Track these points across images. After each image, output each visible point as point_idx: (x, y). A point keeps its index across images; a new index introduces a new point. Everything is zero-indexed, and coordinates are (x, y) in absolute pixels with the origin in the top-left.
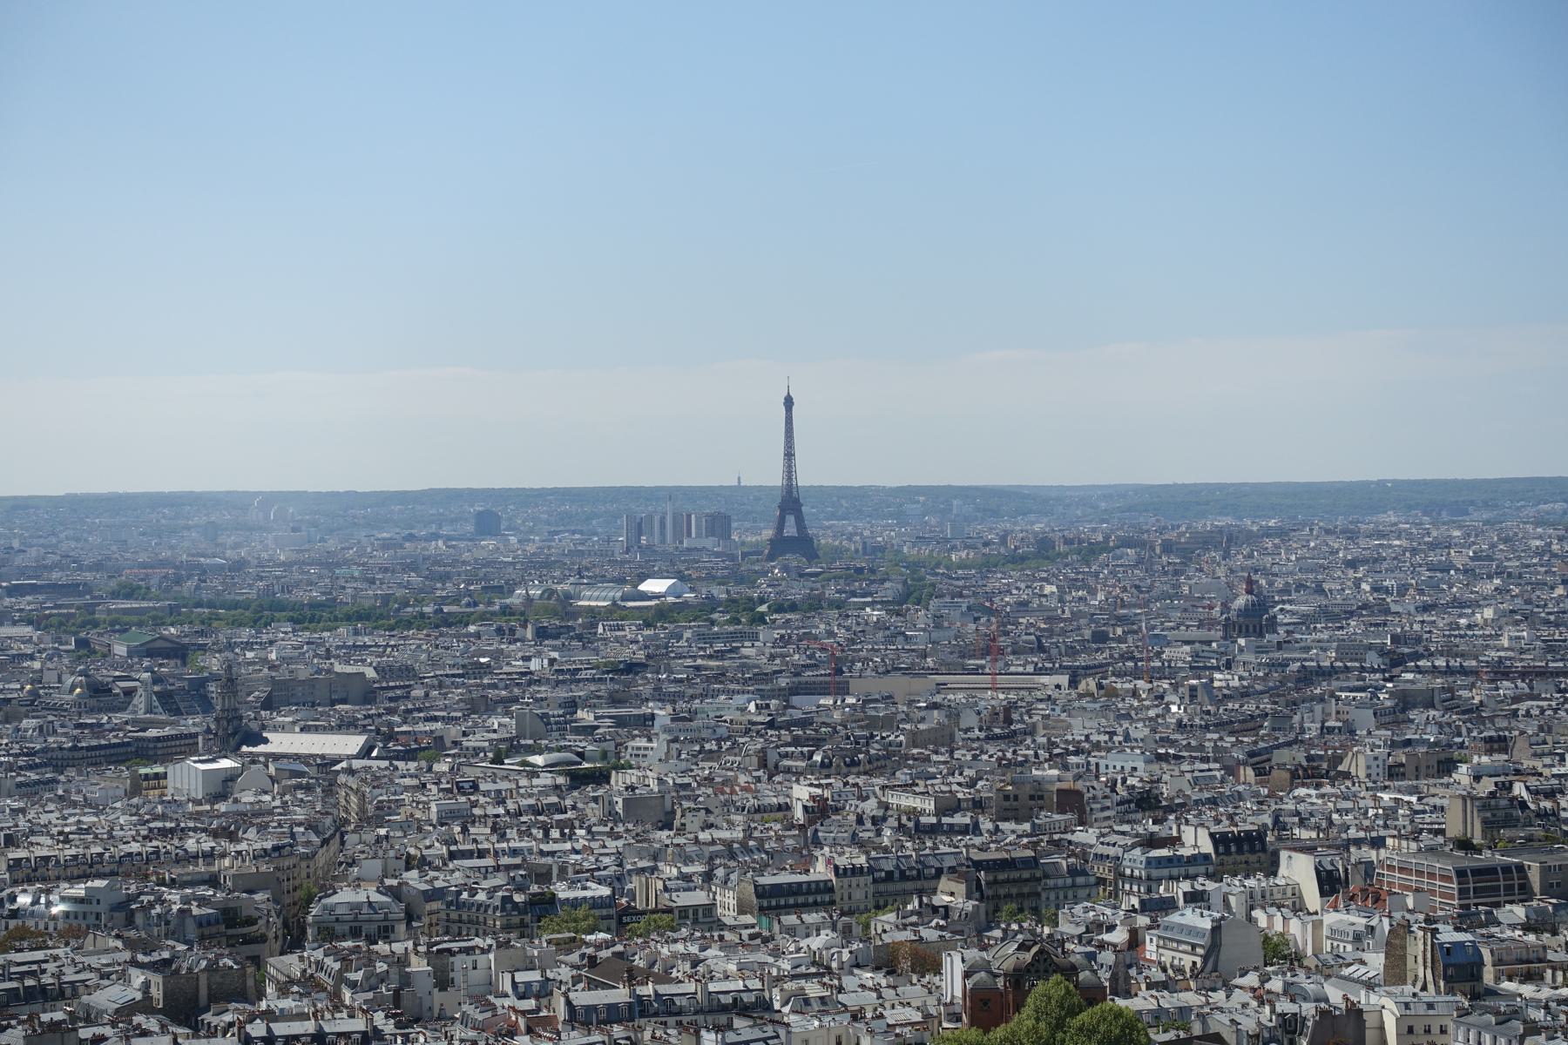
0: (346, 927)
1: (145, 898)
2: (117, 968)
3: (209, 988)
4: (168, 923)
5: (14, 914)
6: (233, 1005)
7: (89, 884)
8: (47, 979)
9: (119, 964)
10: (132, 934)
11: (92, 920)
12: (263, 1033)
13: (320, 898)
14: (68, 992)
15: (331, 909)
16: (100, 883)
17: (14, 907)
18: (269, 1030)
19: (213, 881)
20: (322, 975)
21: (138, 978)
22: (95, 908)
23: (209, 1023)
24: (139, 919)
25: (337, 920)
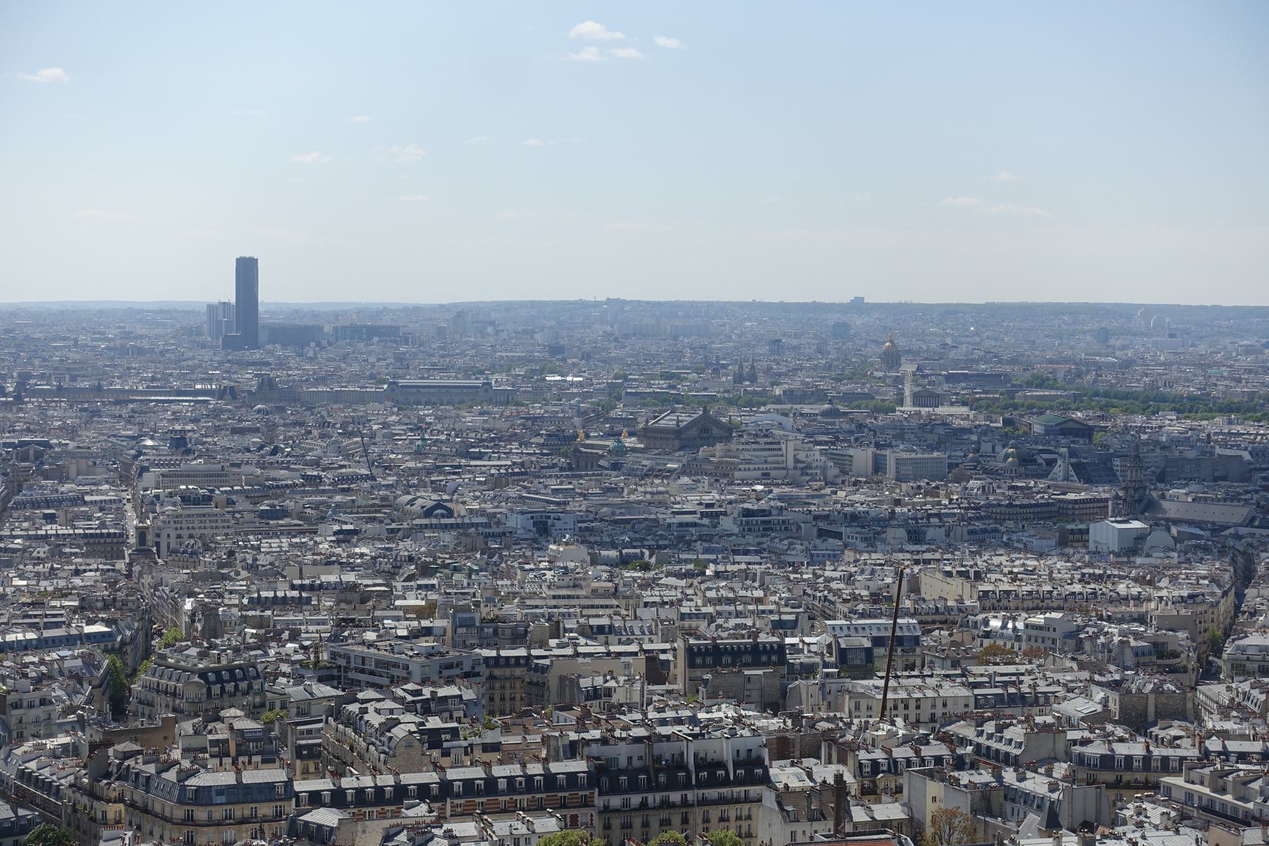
0: (1256, 666)
1: (1091, 630)
2: (1080, 684)
3: (1156, 707)
4: (1110, 651)
5: (987, 635)
6: (1176, 723)
7: (1048, 615)
8: (1025, 689)
9: (1081, 681)
10: (1083, 657)
11: (1049, 643)
12: (1220, 748)
13: (1234, 640)
14: (1042, 700)
15: (1243, 650)
16: (1056, 615)
17: (989, 629)
18: (1224, 746)
19: (1142, 619)
20: (1249, 704)
21: (1099, 694)
22: (1051, 634)
23: (1157, 736)
24: (1087, 646)
25: (1248, 659)
